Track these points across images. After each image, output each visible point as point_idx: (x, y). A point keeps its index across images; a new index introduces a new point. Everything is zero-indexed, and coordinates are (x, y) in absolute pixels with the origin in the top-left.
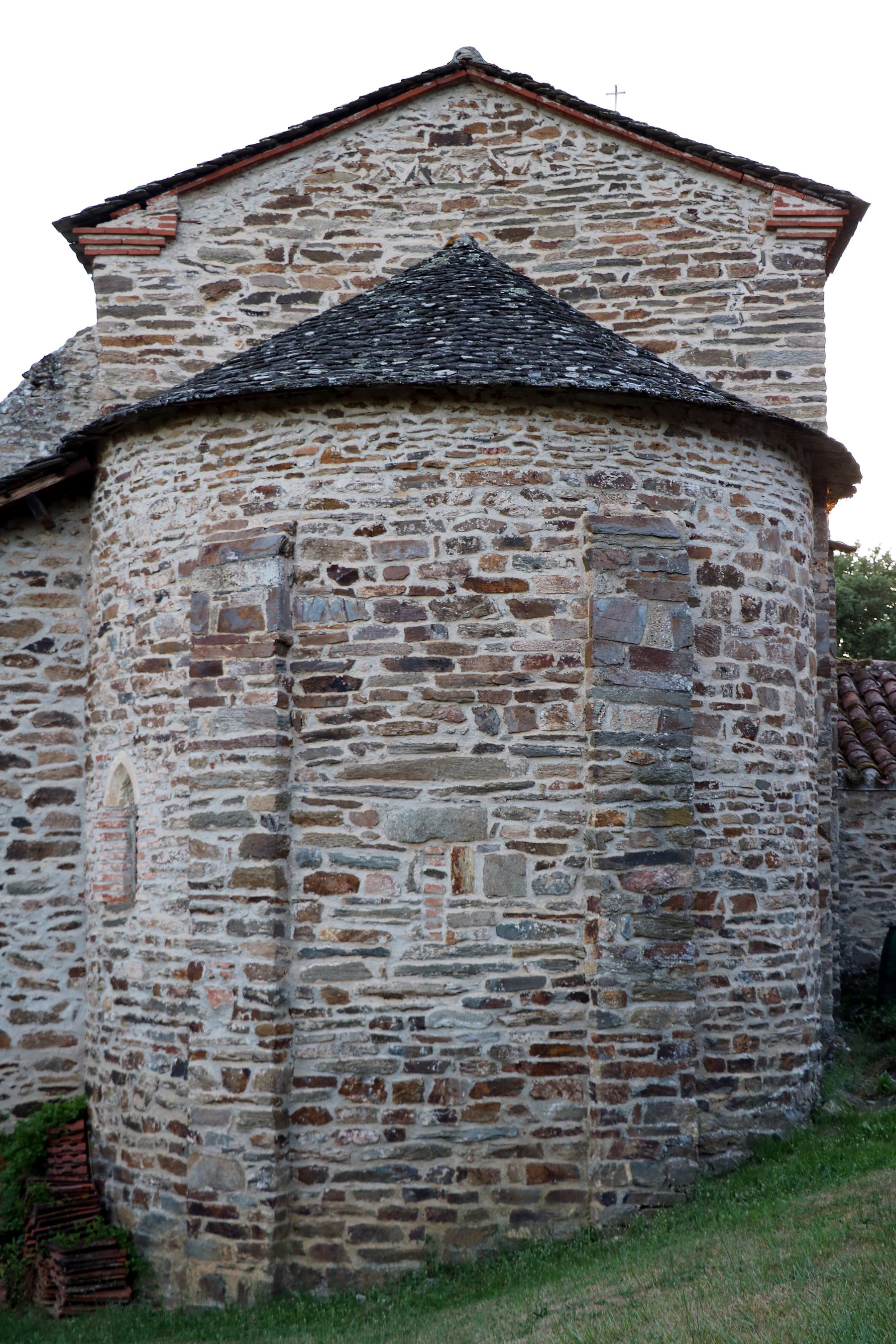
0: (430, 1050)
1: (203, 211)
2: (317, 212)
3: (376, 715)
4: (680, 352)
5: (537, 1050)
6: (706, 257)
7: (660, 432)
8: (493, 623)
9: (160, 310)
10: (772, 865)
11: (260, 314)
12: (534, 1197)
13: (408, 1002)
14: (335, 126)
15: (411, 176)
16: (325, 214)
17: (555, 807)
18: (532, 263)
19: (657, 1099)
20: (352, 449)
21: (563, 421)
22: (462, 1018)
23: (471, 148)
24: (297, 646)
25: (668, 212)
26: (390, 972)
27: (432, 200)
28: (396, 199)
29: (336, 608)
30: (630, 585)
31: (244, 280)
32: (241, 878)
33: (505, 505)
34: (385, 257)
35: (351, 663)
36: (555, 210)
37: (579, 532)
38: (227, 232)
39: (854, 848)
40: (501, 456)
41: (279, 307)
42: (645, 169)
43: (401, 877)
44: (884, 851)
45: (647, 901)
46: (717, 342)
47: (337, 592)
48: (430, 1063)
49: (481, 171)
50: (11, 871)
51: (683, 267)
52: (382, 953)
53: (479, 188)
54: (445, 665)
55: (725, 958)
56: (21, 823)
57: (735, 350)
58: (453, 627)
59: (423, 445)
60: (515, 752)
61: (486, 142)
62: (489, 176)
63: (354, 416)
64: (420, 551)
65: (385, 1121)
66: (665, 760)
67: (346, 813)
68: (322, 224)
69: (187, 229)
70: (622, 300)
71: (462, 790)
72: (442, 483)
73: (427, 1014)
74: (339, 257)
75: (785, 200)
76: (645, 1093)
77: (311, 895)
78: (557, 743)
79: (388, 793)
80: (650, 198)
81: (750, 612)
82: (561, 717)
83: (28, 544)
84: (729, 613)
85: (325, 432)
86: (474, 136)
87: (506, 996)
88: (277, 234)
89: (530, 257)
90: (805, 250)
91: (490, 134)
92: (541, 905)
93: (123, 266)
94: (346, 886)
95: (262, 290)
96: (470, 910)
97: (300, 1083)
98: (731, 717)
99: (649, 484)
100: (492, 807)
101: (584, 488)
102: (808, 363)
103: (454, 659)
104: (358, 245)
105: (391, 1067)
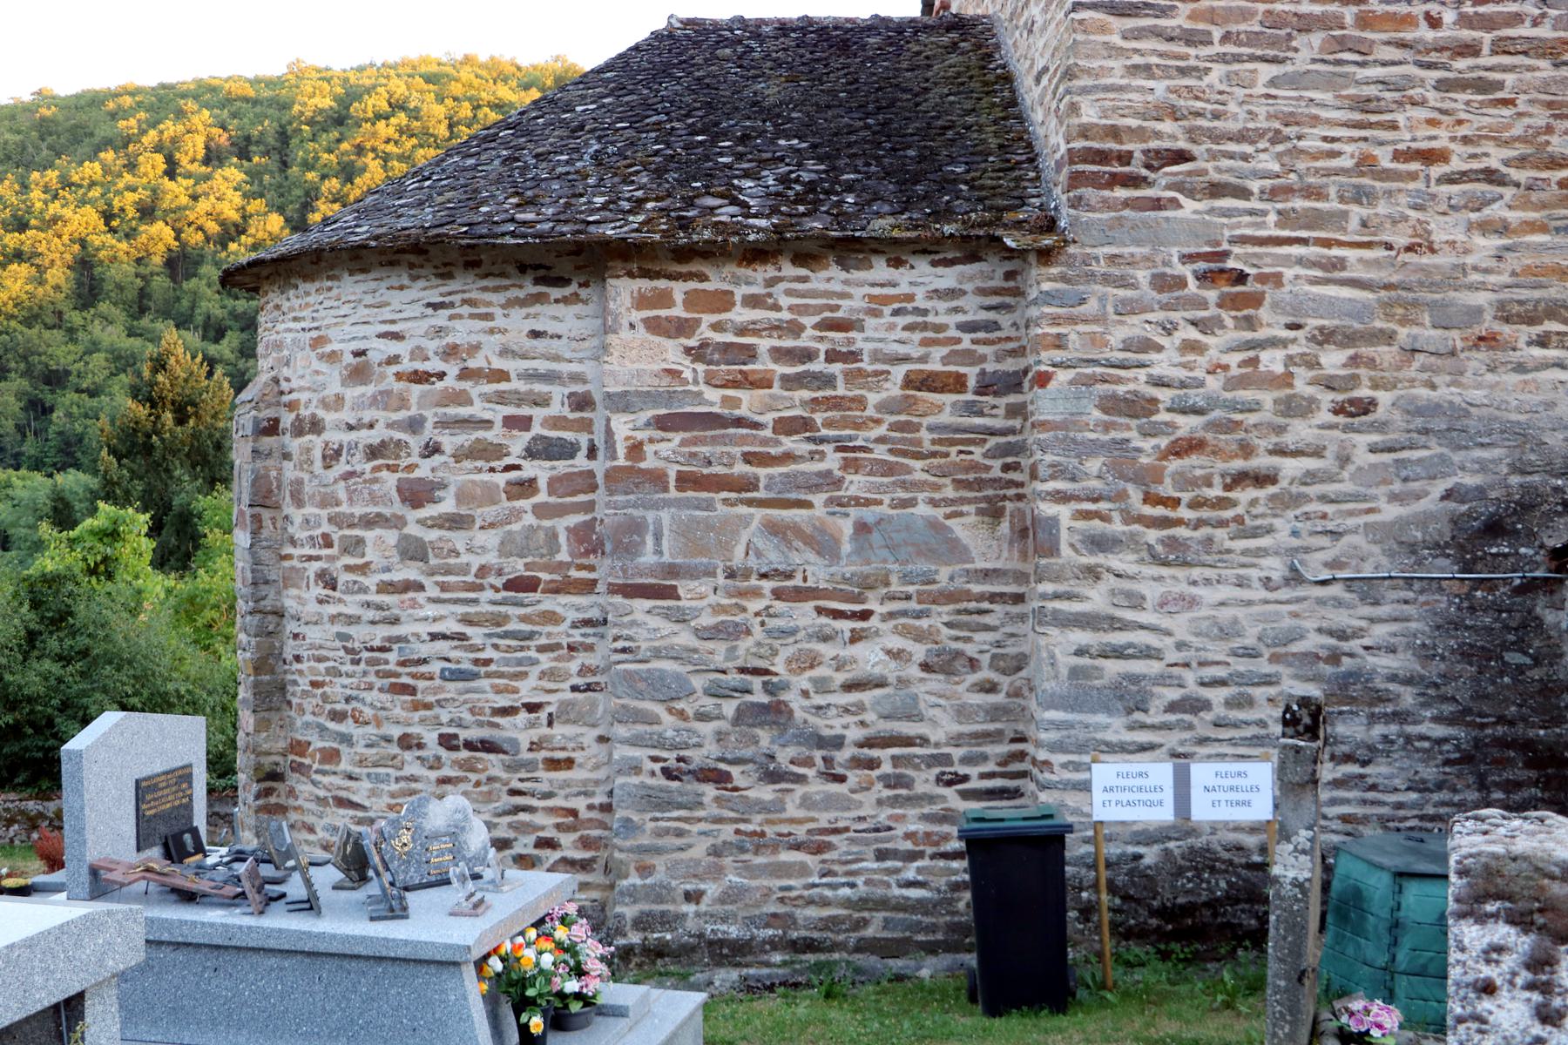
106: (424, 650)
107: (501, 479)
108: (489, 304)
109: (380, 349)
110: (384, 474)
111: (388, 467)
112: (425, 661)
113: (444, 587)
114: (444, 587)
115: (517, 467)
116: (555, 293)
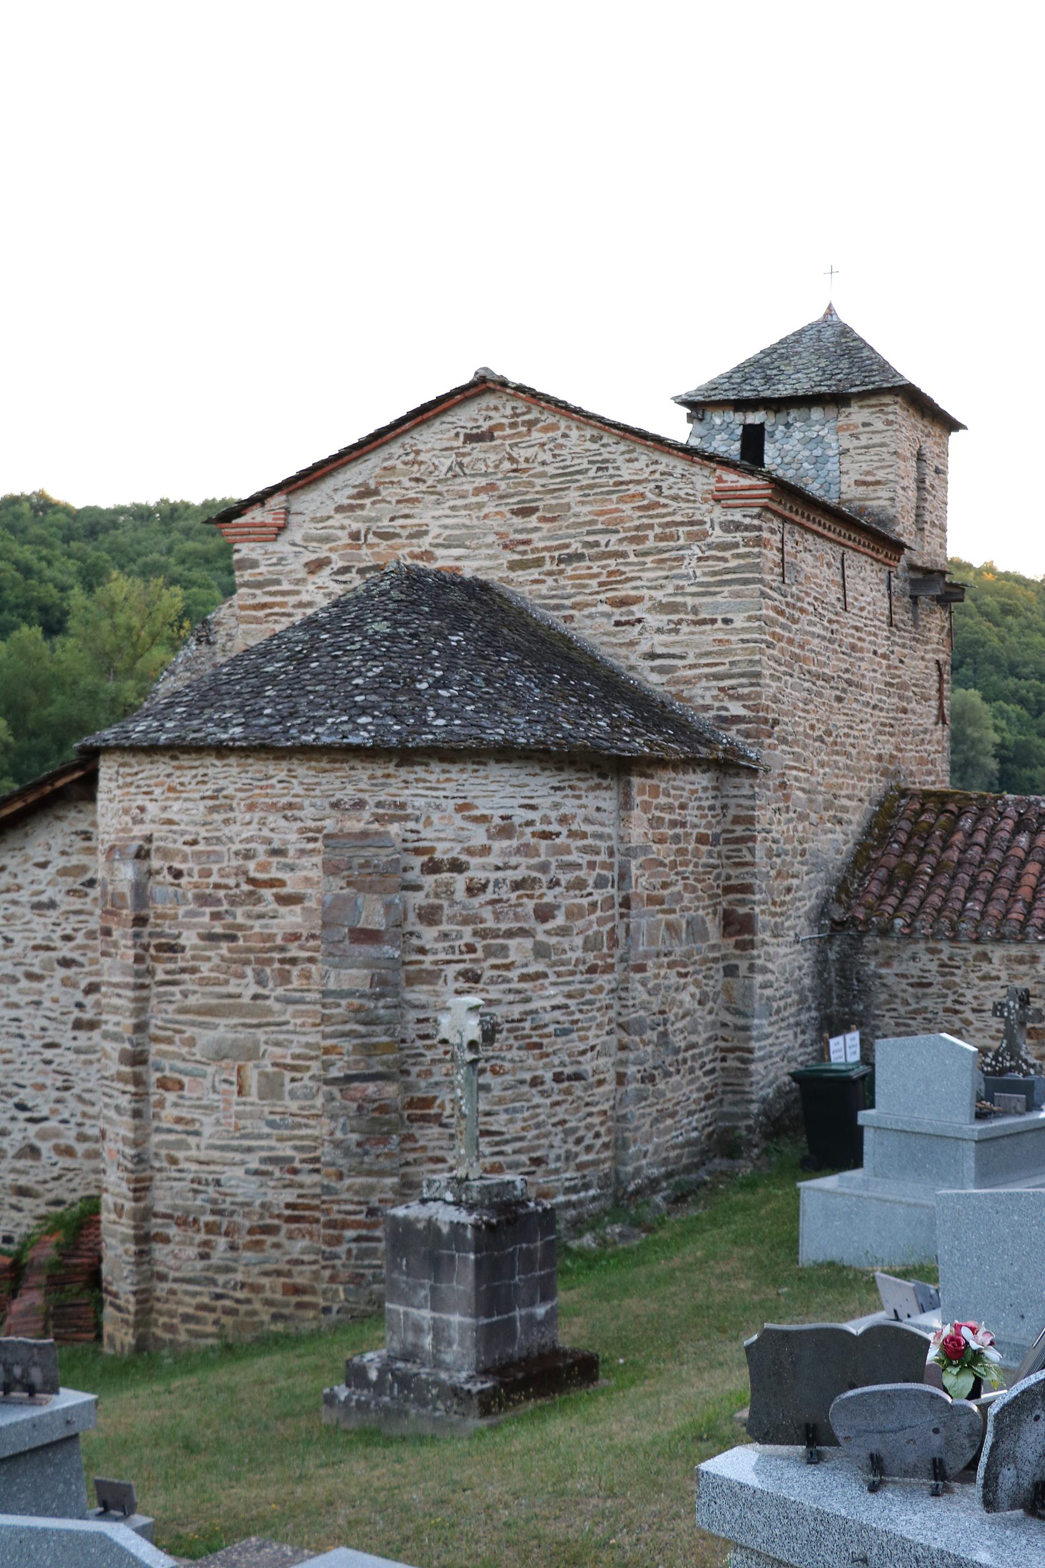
0: (224, 1202)
1: (306, 505)
2: (384, 501)
3: (193, 970)
4: (648, 604)
5: (288, 1206)
6: (668, 525)
7: (392, 765)
8: (263, 910)
9: (278, 582)
10: (495, 1072)
11: (345, 582)
12: (286, 1305)
13: (212, 1168)
14: (392, 434)
15: (450, 469)
16: (389, 502)
17: (304, 1039)
18: (539, 534)
19: (365, 1245)
20: (182, 784)
21: (313, 764)
22: (244, 1181)
23: (493, 443)
24: (152, 920)
25: (640, 489)
26: (202, 1146)
27: (466, 487)
28: (440, 488)
29: (171, 895)
30: (349, 884)
31: (334, 556)
32: (120, 1077)
33: (272, 826)
34: (431, 534)
35: (179, 936)
36: (555, 490)
37: (319, 845)
38: (323, 520)
39: (884, 985)
40: (269, 791)
41: (358, 576)
42: (623, 453)
43: (207, 1083)
44: (910, 989)
45: (360, 1108)
46: (675, 594)
47: (172, 884)
48: (224, 1210)
49: (501, 461)
50: (75, 1038)
51: (651, 534)
52: (197, 1133)
53: (500, 476)
54: (233, 938)
55: (444, 1143)
56: (80, 1006)
57: (690, 601)
58: (239, 911)
59: (222, 783)
60: (277, 1000)
61: (504, 438)
62: (507, 465)
63: (185, 761)
64: (218, 857)
65: (199, 1246)
66: (376, 1008)
67: (177, 1038)
68: (388, 509)
69: (293, 519)
70: (604, 562)
71: (244, 1025)
72: (232, 809)
73: (222, 1177)
74: (398, 535)
75: (725, 477)
76: (358, 1239)
77: (161, 1091)
78: (305, 994)
79: (201, 1025)
80: (627, 478)
81: (472, 890)
82: (307, 976)
83: (80, 812)
84: (453, 893)
85: (169, 770)
86: (496, 434)
87: (270, 1168)
88: (356, 520)
89: (537, 529)
90: (744, 516)
91: (508, 431)
92: (294, 1106)
93: (253, 550)
94: (177, 1087)
95: (346, 564)
96: (248, 1108)
97: (156, 1215)
98: (451, 970)
99: (379, 805)
100: (263, 1038)
101: (328, 811)
102: (746, 611)
103: (239, 934)
104: (412, 526)
105: (202, 1211)
106: (547, 1017)
107: (585, 902)
108: (580, 789)
109: (521, 816)
110: (525, 900)
111: (528, 896)
112: (546, 1026)
113: (559, 975)
114: (559, 975)
115: (590, 894)
116: (605, 783)
